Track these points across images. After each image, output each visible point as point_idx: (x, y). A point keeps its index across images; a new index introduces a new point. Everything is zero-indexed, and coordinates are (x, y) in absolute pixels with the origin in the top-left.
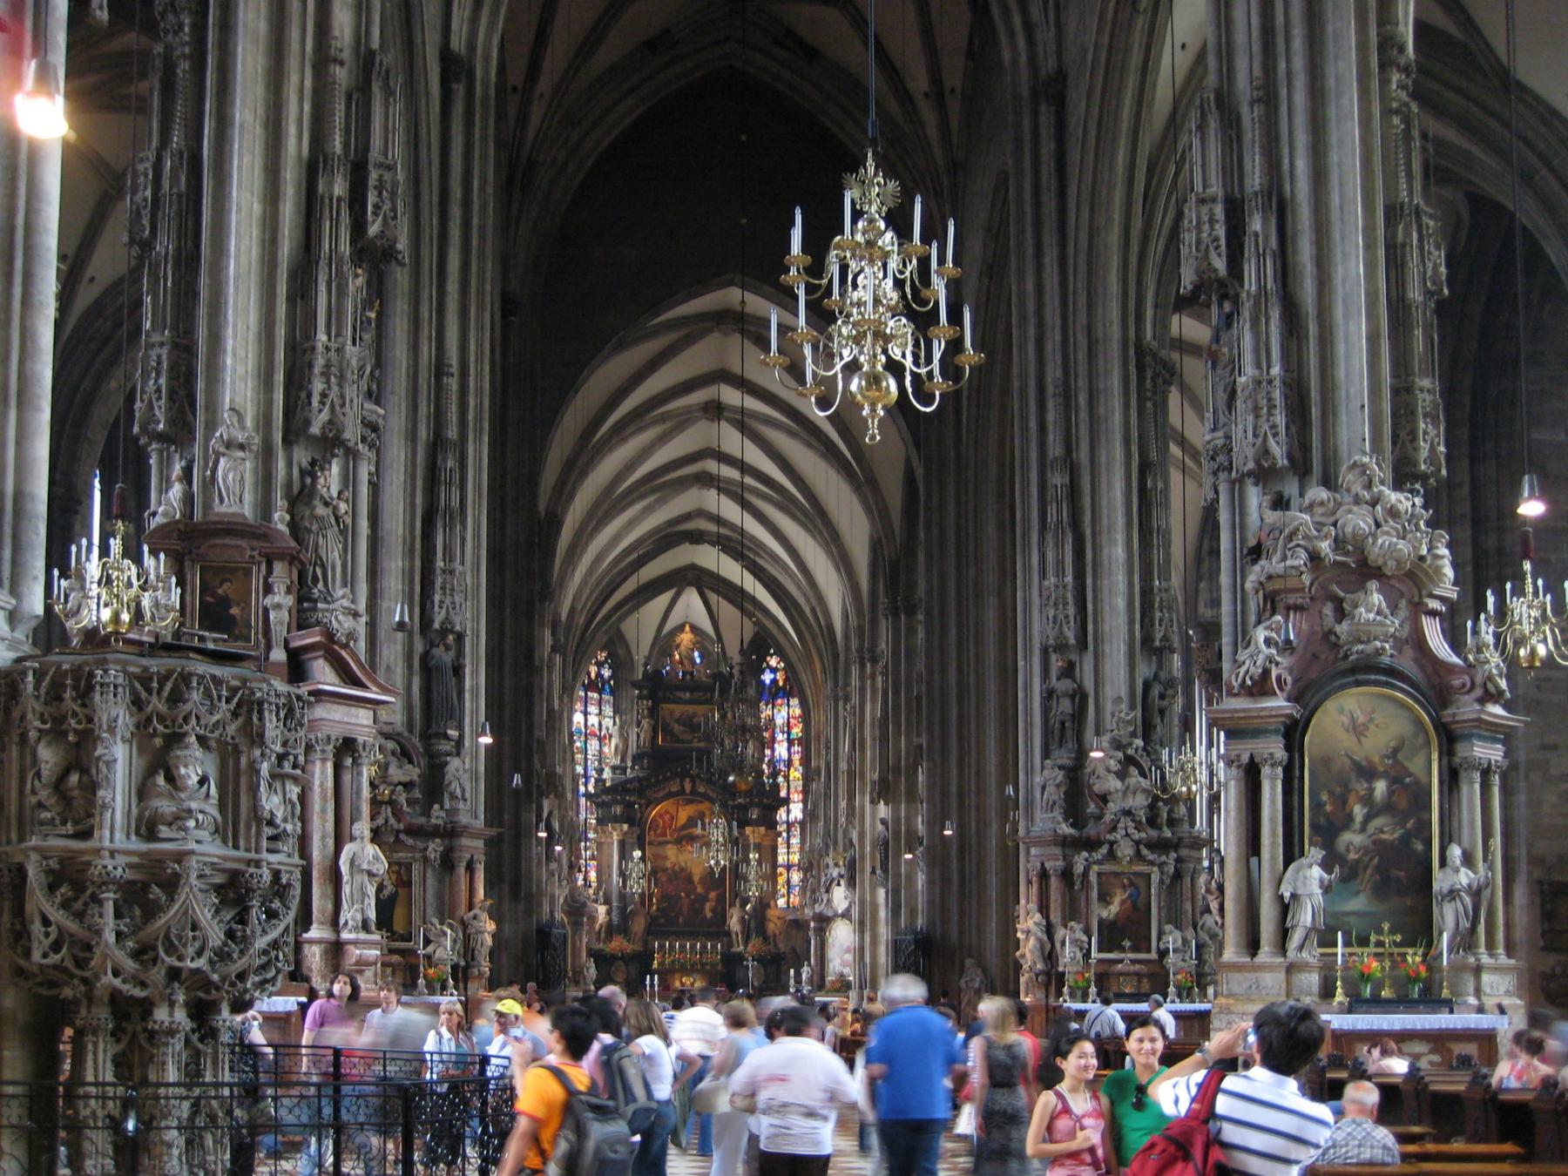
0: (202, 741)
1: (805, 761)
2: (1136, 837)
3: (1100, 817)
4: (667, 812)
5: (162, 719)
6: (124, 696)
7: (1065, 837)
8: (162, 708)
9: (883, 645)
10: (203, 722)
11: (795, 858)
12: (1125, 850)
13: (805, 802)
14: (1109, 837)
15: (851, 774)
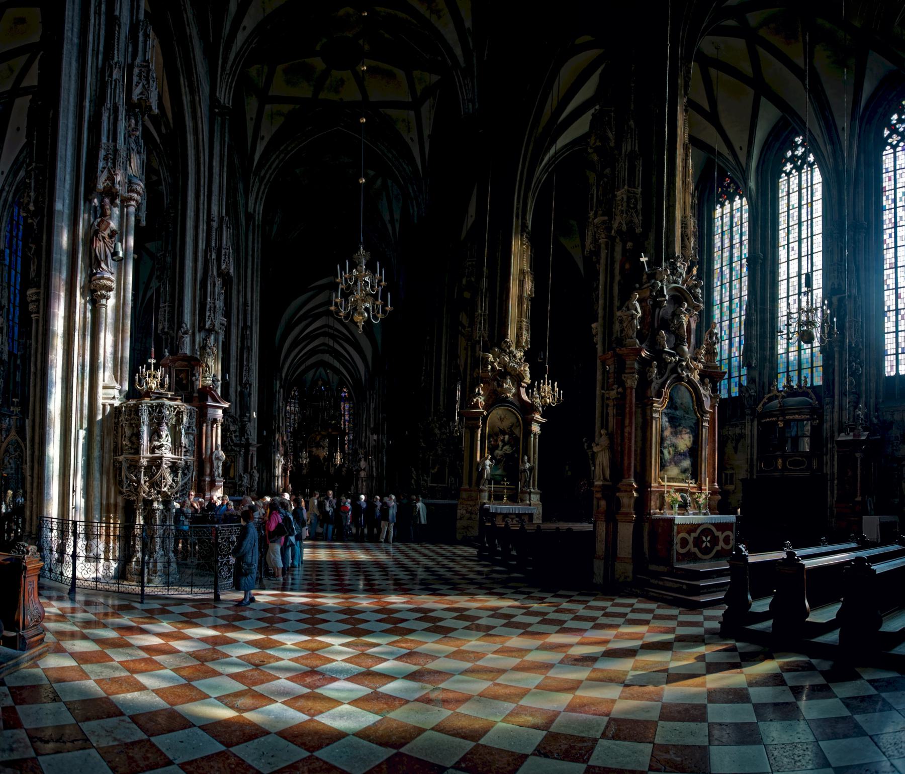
0: (167, 424)
6: (147, 412)
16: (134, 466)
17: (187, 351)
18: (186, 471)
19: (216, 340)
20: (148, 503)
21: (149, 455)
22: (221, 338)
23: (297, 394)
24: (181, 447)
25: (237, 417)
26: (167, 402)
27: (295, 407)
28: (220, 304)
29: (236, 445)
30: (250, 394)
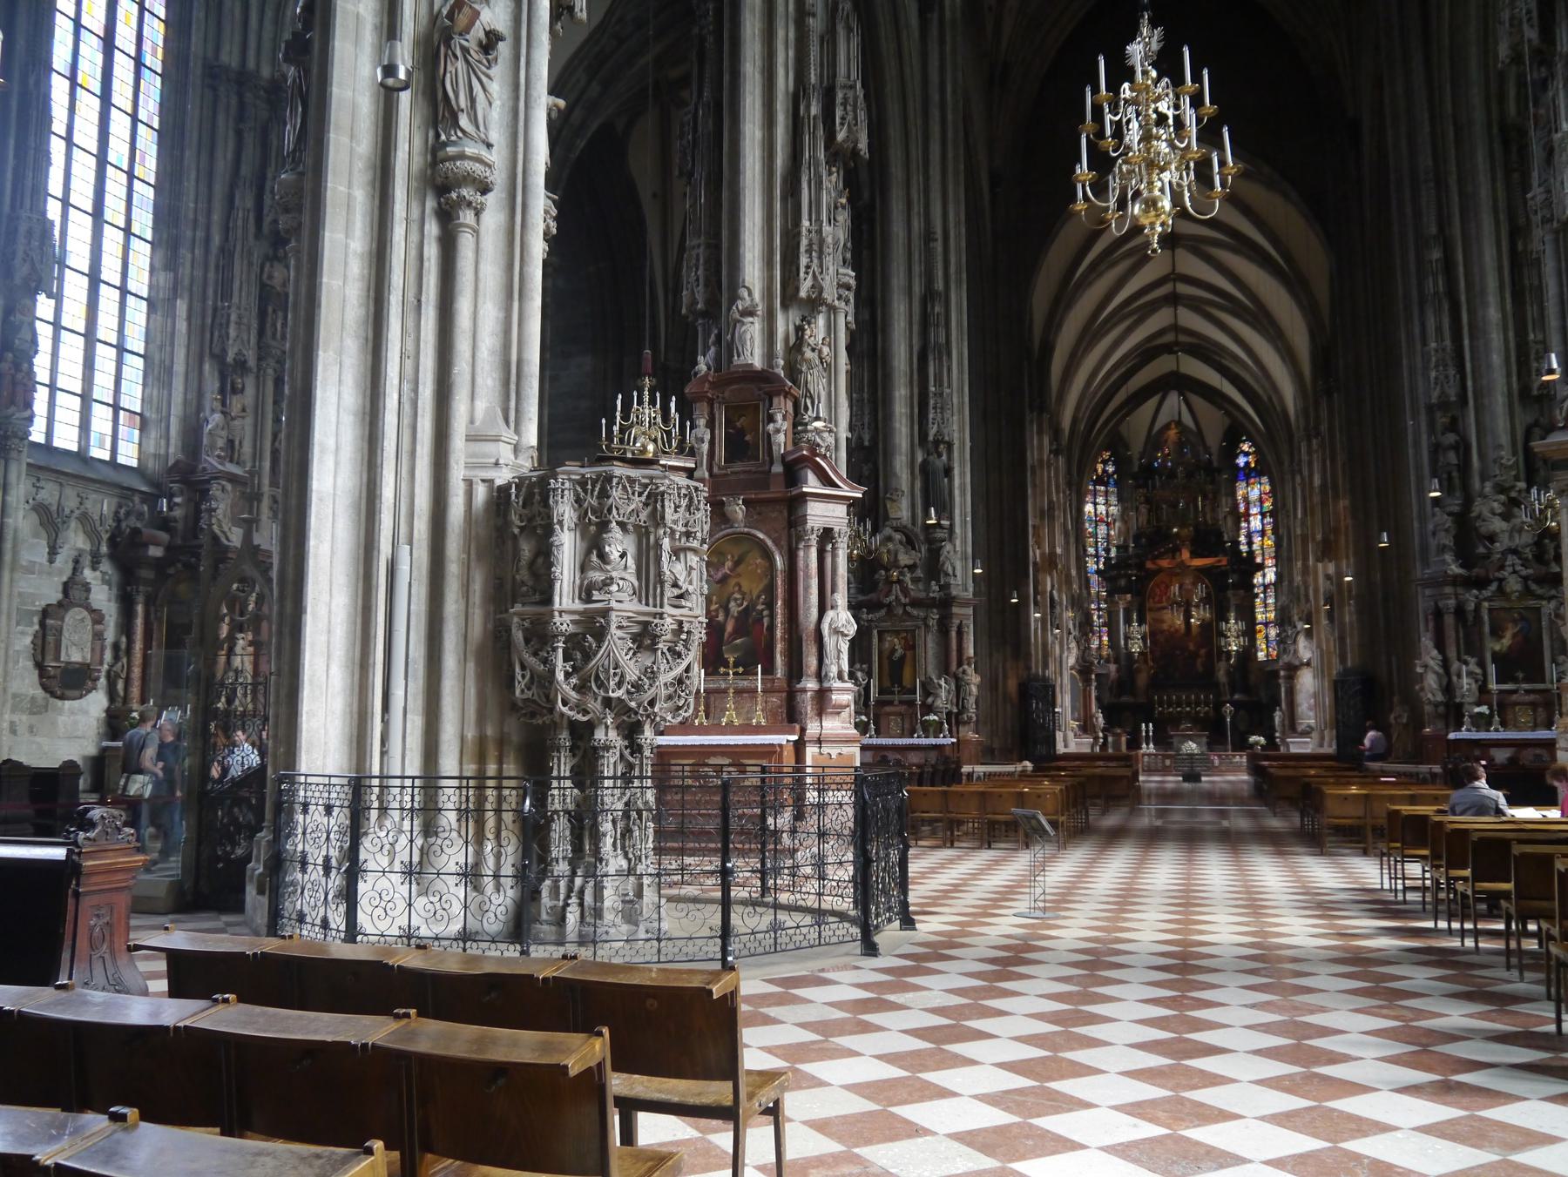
0: (622, 525)
1: (1275, 531)
2: (1524, 572)
3: (1487, 556)
4: (1163, 582)
5: (594, 512)
6: (569, 496)
7: (1456, 577)
8: (594, 502)
9: (1324, 428)
10: (621, 512)
11: (1272, 616)
12: (1513, 585)
13: (1276, 566)
14: (1497, 574)
15: (1305, 539)
16: (540, 635)
17: (753, 355)
18: (679, 648)
19: (831, 328)
20: (582, 732)
21: (579, 606)
22: (845, 319)
23: (1111, 469)
24: (662, 583)
25: (918, 530)
26: (619, 470)
27: (1107, 504)
28: (836, 232)
29: (916, 603)
30: (948, 471)
